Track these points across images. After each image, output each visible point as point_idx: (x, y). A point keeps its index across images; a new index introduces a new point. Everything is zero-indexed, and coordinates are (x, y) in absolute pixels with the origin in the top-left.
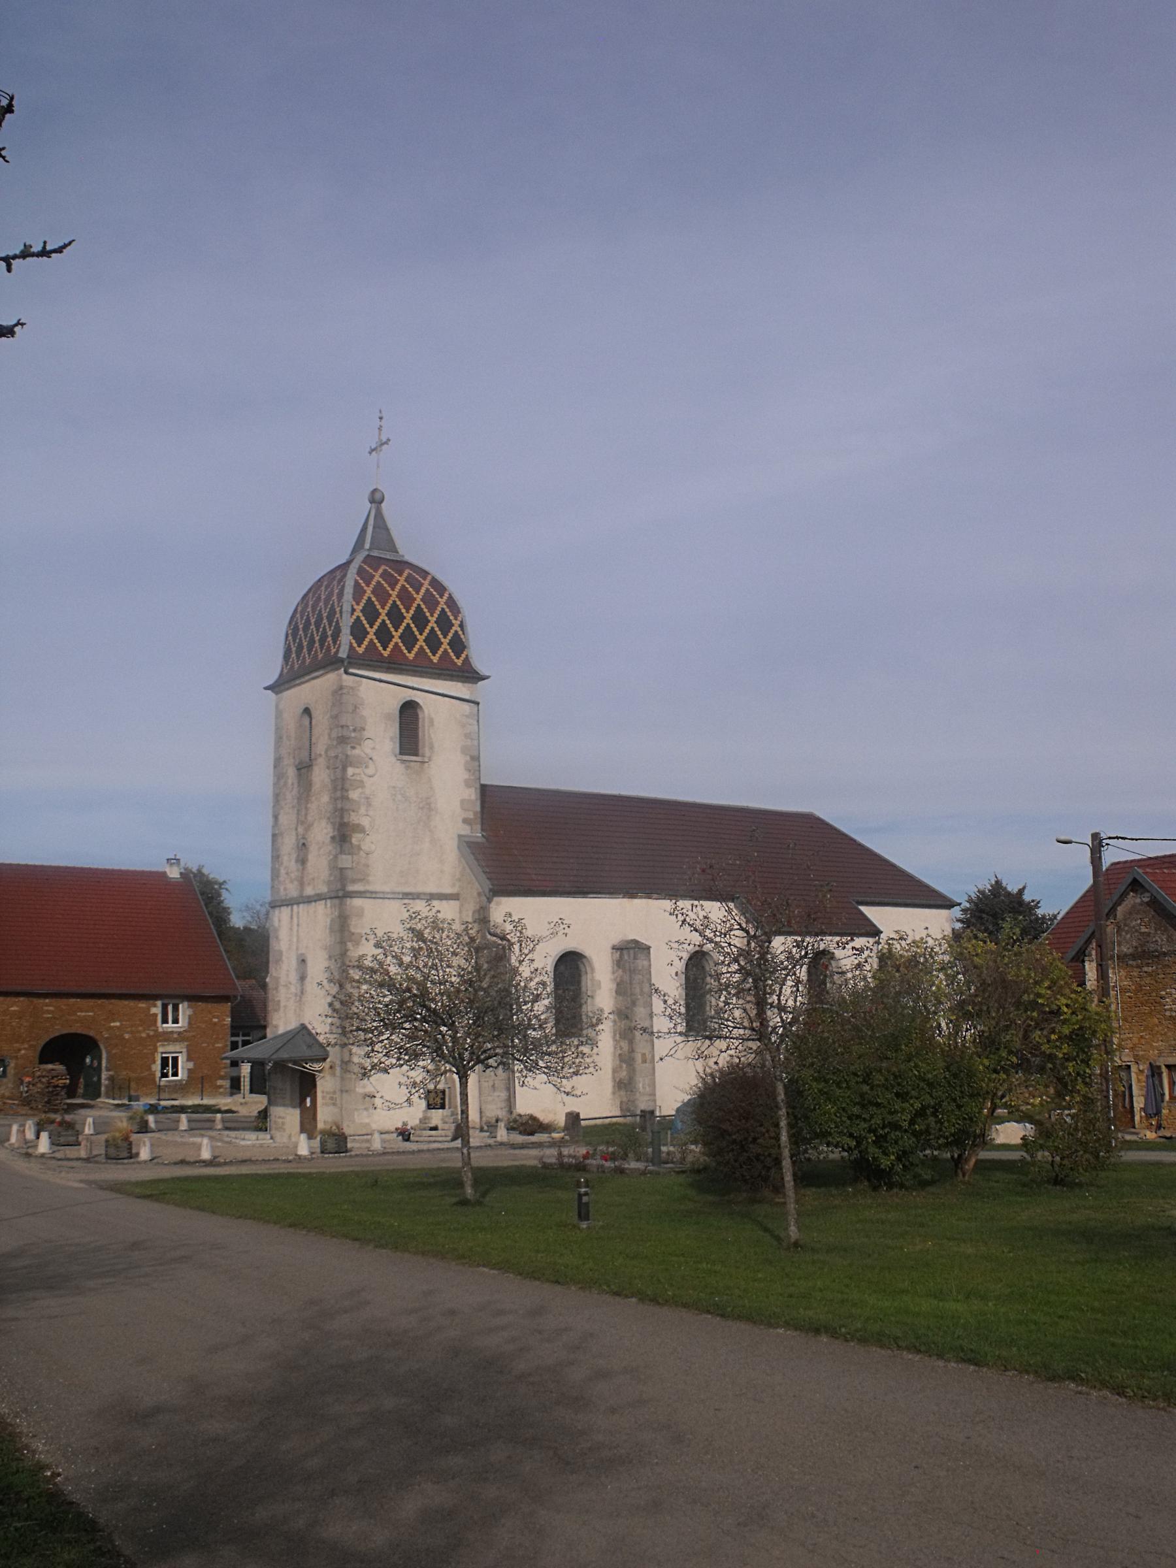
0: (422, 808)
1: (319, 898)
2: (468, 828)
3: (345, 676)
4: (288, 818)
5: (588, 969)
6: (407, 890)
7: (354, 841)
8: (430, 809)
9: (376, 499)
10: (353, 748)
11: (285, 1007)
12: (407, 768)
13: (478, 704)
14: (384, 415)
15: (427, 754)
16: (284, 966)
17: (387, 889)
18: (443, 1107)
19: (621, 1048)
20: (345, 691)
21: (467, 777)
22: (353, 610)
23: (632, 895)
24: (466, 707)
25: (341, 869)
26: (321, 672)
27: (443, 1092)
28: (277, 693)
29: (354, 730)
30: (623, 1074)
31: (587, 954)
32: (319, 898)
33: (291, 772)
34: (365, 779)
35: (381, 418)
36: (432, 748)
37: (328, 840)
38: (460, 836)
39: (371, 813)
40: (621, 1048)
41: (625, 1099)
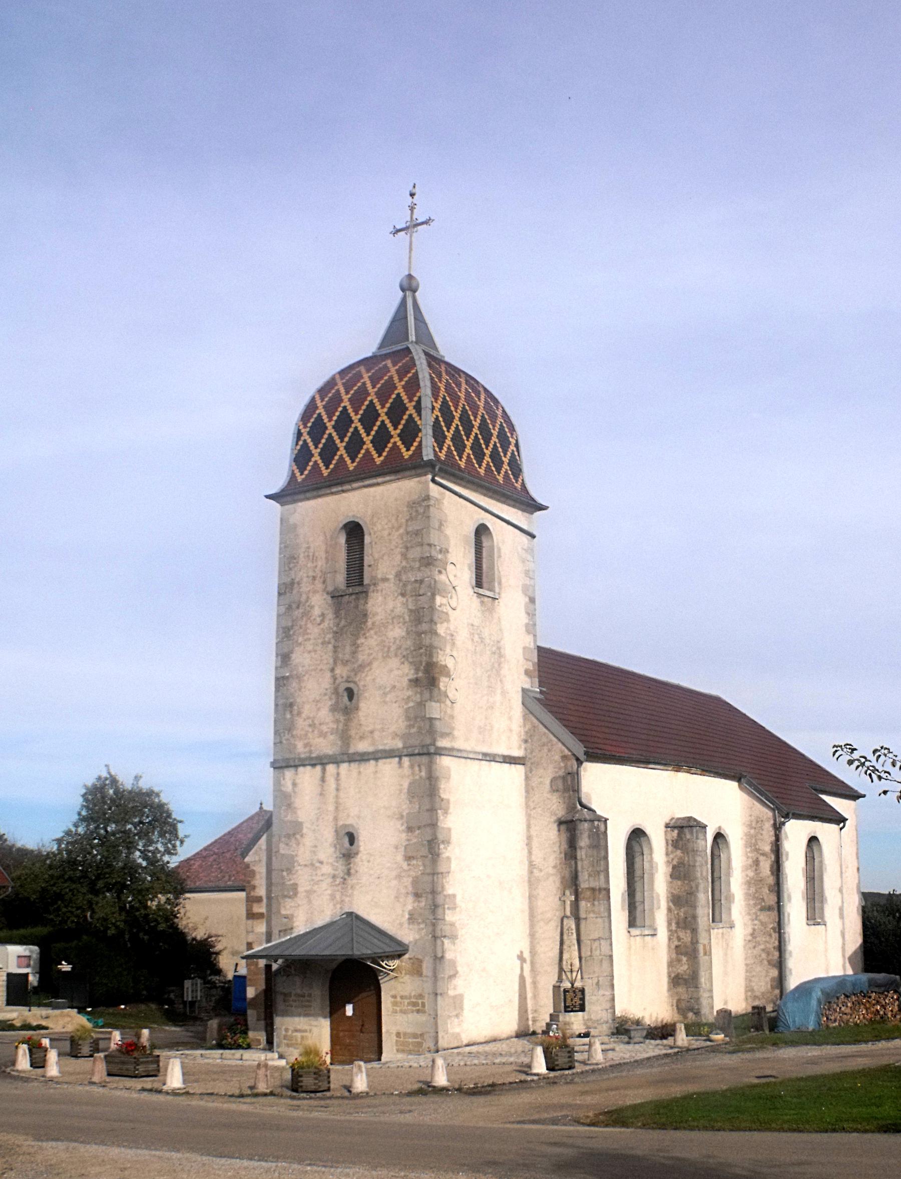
0: (494, 653)
1: (389, 754)
2: (528, 680)
3: (432, 485)
6: (489, 751)
8: (501, 656)
9: (409, 286)
10: (440, 572)
11: (309, 893)
12: (482, 602)
13: (533, 537)
14: (417, 190)
15: (497, 590)
16: (308, 841)
17: (469, 749)
18: (582, 1009)
19: (679, 939)
20: (432, 502)
21: (527, 621)
22: (433, 408)
23: (678, 768)
25: (431, 719)
26: (393, 477)
27: (583, 991)
28: (282, 504)
29: (441, 551)
30: (683, 968)
31: (647, 832)
32: (389, 754)
33: (319, 603)
34: (450, 612)
35: (412, 195)
36: (500, 583)
37: (405, 682)
38: (524, 690)
39: (455, 654)
41: (685, 996)
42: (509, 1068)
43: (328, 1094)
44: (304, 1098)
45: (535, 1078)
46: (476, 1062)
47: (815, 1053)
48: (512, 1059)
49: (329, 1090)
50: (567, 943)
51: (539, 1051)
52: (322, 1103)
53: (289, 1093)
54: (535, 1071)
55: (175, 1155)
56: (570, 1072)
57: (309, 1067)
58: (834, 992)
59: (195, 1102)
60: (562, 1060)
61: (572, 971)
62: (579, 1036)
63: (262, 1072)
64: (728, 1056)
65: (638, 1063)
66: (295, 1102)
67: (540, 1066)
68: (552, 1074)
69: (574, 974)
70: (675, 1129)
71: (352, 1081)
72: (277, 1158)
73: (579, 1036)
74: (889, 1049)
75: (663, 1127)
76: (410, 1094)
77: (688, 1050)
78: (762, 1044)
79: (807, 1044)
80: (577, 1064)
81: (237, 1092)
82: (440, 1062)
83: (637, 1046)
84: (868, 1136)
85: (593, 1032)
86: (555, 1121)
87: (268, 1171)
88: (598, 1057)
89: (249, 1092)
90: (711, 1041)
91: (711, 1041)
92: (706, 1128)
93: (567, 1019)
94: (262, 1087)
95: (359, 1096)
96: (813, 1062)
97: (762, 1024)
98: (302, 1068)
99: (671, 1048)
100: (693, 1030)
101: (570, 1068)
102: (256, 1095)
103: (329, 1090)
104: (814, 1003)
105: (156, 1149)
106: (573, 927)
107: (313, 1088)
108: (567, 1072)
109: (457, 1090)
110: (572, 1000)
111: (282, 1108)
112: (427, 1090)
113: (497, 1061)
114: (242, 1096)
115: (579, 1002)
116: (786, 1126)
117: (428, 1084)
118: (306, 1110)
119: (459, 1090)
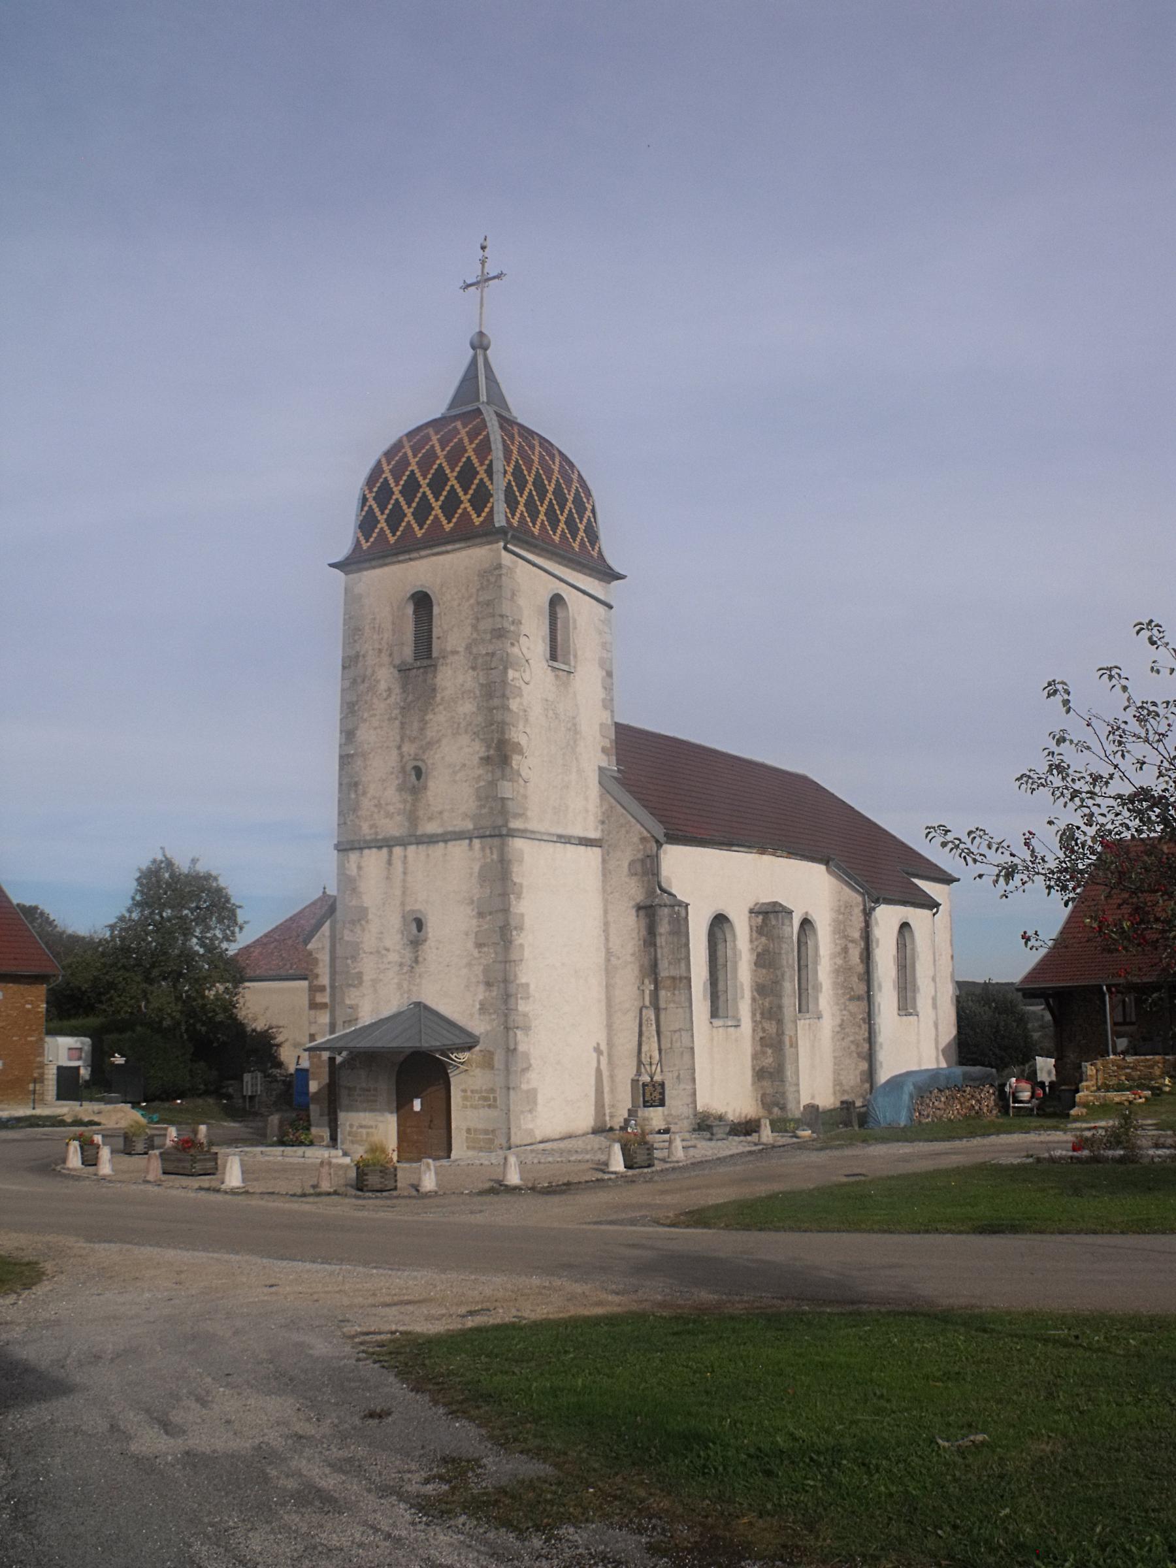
1: (458, 836)
2: (605, 757)
3: (504, 553)
4: (376, 733)
5: (729, 937)
7: (514, 763)
8: (576, 732)
9: (480, 344)
10: (512, 644)
11: (375, 982)
12: (557, 676)
13: (611, 607)
14: (488, 243)
15: (572, 663)
17: (543, 830)
18: (662, 1104)
19: (764, 1030)
20: (504, 571)
21: (603, 696)
22: (505, 472)
23: (762, 851)
24: (602, 609)
25: (503, 799)
26: (462, 545)
27: (662, 1085)
28: (346, 573)
29: (513, 623)
30: (769, 1061)
31: (730, 918)
32: (458, 836)
33: (385, 677)
34: (523, 686)
35: (483, 248)
36: (575, 656)
38: (601, 769)
39: (528, 730)
40: (764, 1030)
41: (770, 1091)
42: (585, 1166)
43: (395, 1193)
44: (370, 1198)
45: (613, 1176)
46: (550, 1159)
47: (907, 1151)
48: (588, 1157)
49: (395, 1189)
50: (646, 1034)
51: (617, 1148)
52: (389, 1202)
53: (354, 1192)
54: (612, 1169)
55: (233, 1257)
56: (649, 1170)
57: (374, 1165)
58: (926, 1086)
59: (254, 1202)
60: (641, 1158)
61: (651, 1064)
62: (659, 1132)
63: (325, 1170)
64: (815, 1153)
65: (721, 1161)
66: (360, 1202)
67: (617, 1164)
68: (630, 1172)
69: (654, 1067)
70: (760, 1230)
71: (420, 1179)
72: (341, 1261)
73: (659, 1132)
74: (984, 1146)
75: (747, 1228)
76: (482, 1193)
77: (773, 1147)
78: (851, 1141)
79: (898, 1141)
80: (656, 1162)
81: (299, 1191)
82: (512, 1160)
83: (720, 1143)
84: (963, 1237)
85: (673, 1128)
86: (633, 1222)
87: (331, 1274)
88: (679, 1154)
89: (312, 1191)
90: (797, 1137)
91: (797, 1137)
92: (792, 1229)
93: (646, 1114)
94: (325, 1186)
95: (427, 1195)
96: (905, 1159)
97: (851, 1120)
98: (368, 1166)
99: (756, 1144)
100: (776, 1126)
101: (649, 1166)
102: (319, 1194)
103: (395, 1189)
104: (906, 1097)
105: (214, 1252)
106: (653, 1017)
107: (379, 1187)
108: (646, 1170)
109: (530, 1189)
110: (651, 1094)
111: (346, 1208)
112: (499, 1189)
113: (572, 1158)
114: (304, 1195)
115: (658, 1097)
116: (876, 1227)
117: (500, 1183)
118: (372, 1210)
119: (533, 1189)
